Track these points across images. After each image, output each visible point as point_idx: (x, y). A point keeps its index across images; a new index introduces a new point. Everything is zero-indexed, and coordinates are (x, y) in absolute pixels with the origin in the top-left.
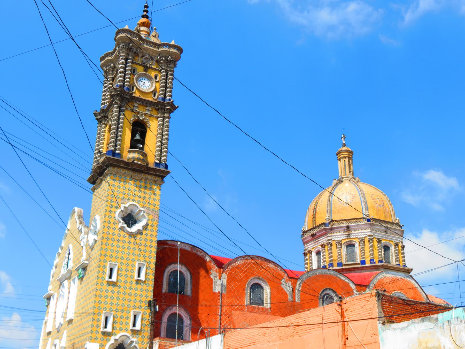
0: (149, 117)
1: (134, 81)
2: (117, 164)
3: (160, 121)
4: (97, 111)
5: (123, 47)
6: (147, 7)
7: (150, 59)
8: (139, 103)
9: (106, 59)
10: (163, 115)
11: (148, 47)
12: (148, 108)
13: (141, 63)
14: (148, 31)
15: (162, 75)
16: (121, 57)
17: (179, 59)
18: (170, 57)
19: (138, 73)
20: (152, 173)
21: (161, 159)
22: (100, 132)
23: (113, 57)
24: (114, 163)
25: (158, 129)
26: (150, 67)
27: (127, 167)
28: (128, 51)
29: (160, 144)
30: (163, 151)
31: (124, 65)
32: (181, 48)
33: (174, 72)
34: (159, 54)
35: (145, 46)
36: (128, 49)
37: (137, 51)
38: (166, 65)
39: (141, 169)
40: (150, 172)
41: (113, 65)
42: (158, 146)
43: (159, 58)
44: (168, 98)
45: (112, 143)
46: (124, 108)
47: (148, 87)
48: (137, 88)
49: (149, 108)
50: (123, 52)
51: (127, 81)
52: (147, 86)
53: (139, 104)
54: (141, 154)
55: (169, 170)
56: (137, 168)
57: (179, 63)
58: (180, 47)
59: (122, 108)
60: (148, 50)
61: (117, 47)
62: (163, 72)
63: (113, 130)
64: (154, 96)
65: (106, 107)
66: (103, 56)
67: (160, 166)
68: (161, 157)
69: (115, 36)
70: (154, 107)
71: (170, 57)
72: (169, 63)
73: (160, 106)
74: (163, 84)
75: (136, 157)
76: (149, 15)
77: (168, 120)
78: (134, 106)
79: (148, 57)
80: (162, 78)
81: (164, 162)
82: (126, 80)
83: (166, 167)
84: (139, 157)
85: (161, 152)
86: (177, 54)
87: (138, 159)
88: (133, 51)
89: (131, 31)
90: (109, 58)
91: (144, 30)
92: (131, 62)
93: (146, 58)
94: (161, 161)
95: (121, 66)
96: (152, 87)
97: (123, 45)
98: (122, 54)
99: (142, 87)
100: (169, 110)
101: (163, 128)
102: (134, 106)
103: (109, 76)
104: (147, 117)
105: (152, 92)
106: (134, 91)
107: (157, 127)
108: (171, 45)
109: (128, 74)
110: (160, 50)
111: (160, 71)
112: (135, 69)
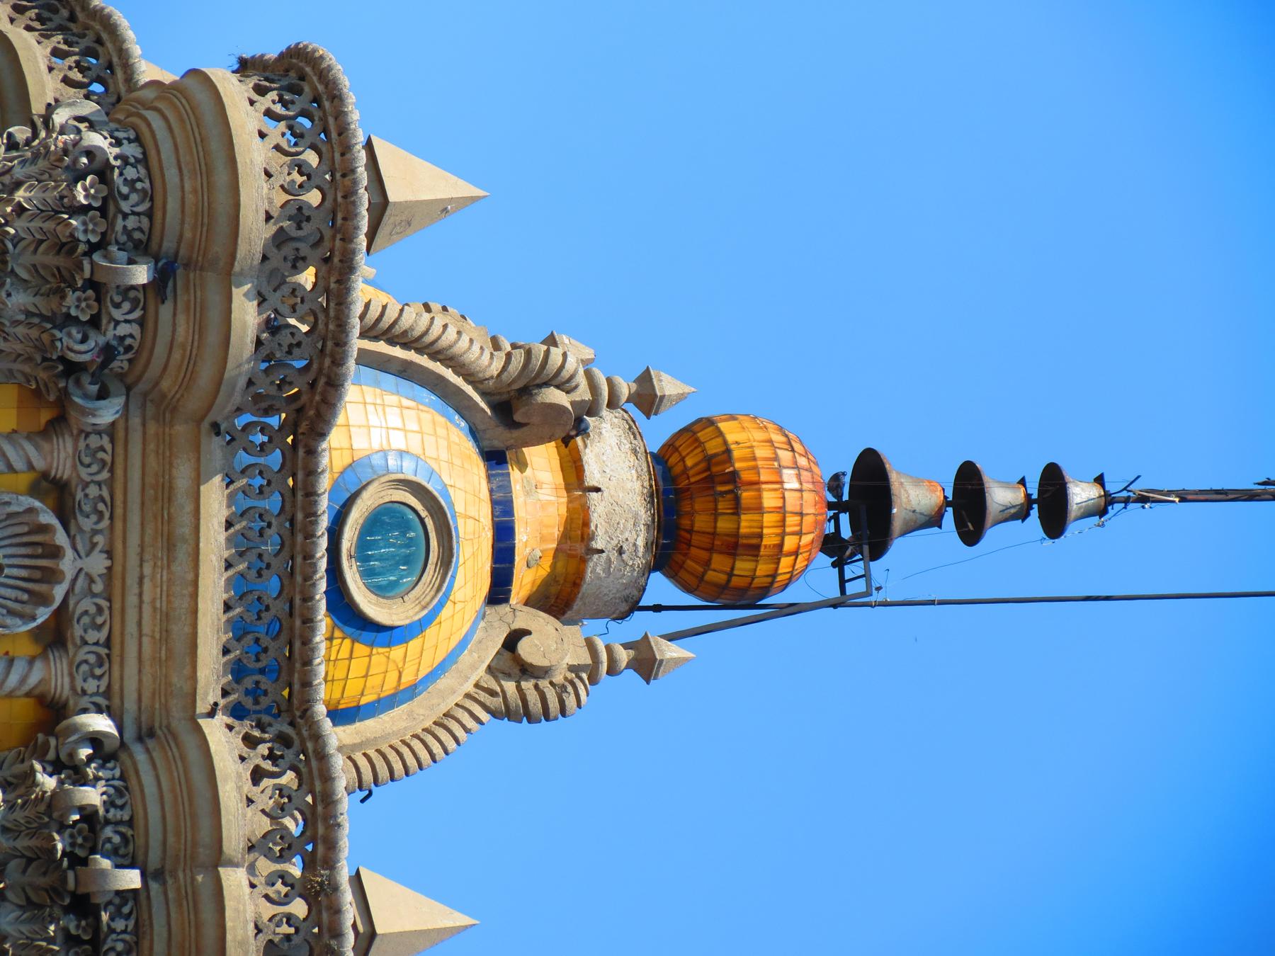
7: (44, 600)
14: (595, 567)
18: (131, 879)
36: (67, 246)
37: (103, 395)
43: (95, 740)
60: (170, 547)
71: (131, 879)
72: (55, 892)
79: (68, 564)
88: (69, 320)
91: (599, 508)
93: (55, 552)
97: (103, 173)
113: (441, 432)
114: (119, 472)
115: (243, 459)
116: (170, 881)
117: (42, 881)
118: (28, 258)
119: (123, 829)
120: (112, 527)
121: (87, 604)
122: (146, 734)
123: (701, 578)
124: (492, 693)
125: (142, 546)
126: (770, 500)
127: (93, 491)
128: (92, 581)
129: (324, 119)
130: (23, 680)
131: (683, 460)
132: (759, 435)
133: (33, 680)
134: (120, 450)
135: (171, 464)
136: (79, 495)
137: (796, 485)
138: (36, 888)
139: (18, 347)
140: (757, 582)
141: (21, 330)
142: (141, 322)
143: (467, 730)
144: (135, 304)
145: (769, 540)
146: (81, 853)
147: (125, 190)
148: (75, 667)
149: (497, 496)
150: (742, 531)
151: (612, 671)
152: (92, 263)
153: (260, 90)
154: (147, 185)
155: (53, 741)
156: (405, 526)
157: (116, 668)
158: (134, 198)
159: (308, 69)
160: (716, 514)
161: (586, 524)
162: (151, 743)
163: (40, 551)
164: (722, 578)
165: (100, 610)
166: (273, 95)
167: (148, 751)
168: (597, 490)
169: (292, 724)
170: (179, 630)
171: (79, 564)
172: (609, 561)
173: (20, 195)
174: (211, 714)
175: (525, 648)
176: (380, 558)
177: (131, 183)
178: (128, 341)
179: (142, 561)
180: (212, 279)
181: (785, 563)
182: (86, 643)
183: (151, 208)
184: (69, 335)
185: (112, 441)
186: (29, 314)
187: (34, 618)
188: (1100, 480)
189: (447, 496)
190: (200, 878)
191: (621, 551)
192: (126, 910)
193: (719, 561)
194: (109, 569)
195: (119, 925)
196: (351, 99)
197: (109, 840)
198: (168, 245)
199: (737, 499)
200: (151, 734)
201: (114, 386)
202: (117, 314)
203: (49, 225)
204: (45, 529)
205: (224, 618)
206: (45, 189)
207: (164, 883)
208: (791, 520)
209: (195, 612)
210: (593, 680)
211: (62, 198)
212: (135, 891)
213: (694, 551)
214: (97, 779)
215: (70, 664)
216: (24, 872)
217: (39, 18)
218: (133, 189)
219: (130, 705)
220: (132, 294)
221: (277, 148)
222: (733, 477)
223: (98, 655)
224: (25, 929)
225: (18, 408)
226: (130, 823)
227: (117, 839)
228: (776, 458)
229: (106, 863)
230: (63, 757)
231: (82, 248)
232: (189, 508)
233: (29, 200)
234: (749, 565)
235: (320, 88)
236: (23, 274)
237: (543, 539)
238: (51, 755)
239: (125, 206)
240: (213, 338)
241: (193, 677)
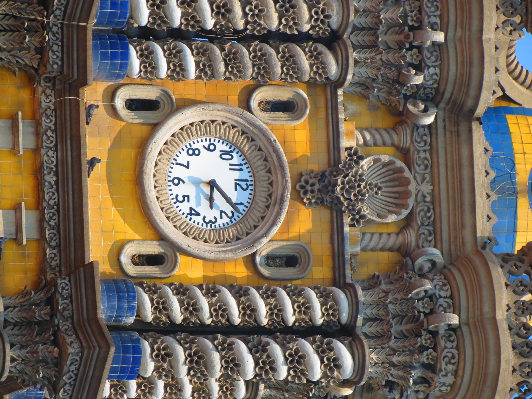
79: (412, 187)
127: (422, 155)
136: (416, 156)
223: (428, 230)
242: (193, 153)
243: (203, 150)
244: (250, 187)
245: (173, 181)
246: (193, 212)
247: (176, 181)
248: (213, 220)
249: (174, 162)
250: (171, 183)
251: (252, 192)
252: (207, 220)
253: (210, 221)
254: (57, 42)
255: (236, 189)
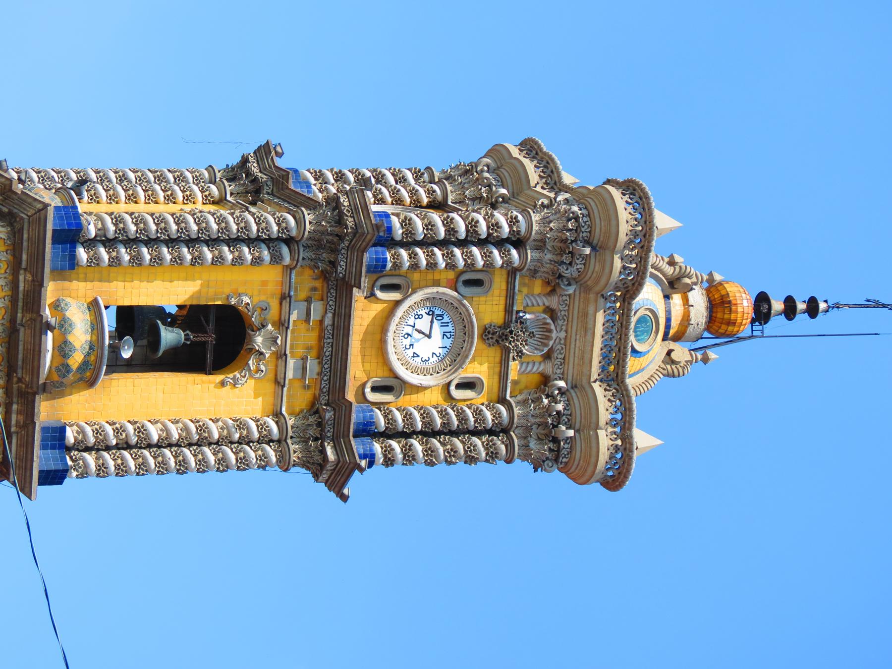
0: (271, 376)
1: (427, 286)
2: (24, 257)
3: (261, 426)
4: (280, 155)
5: (569, 220)
6: (812, 309)
7: (546, 345)
8: (328, 321)
9: (527, 162)
10: (290, 433)
11: (599, 330)
12: (312, 365)
13: (515, 308)
14: (690, 328)
15: (484, 408)
16: (520, 217)
17: (575, 479)
18: (571, 433)
19: (465, 302)
20: (14, 418)
21: (88, 449)
22: (185, 180)
23: (538, 189)
24: (25, 244)
25: (225, 423)
26: (508, 351)
27: (20, 304)
28: (558, 244)
29: (155, 438)
30: (126, 454)
31: (489, 235)
32: (626, 477)
33: (509, 461)
34: (580, 386)
35: (600, 318)
36: (564, 241)
37: (569, 284)
38: (532, 420)
39: (20, 363)
40: (15, 407)
41: (503, 196)
42: (141, 430)
43: (559, 389)
44: (377, 447)
45: (116, 225)
46: (287, 260)
47: (415, 355)
48: (397, 303)
49: (317, 369)
50: (545, 221)
51: (416, 254)
52: (416, 349)
53: (321, 322)
54: (93, 358)
55: (43, 492)
56: (21, 347)
57: (556, 478)
58: (628, 471)
59: (285, 250)
60: (586, 331)
61: (567, 195)
62: (497, 415)
63: (177, 224)
64: (375, 389)
65: (305, 192)
66: (541, 150)
67: (53, 447)
68: (98, 450)
69: (620, 180)
70: (321, 390)
71: (571, 433)
72: (546, 435)
73: (329, 415)
74: (438, 421)
75: (70, 338)
76: (777, 323)
77: (274, 459)
78: (308, 300)
79: (554, 335)
80: (469, 412)
81: (70, 463)
82: (418, 250)
83: (54, 477)
84: (72, 348)
85: (118, 447)
86: (593, 460)
87: (63, 349)
88: (563, 263)
89: (650, 242)
90: (533, 174)
92: (508, 263)
93: (550, 331)
94: (74, 453)
95: (477, 222)
96: (416, 370)
97: (576, 219)
98: (536, 218)
99: (409, 330)
100: (318, 458)
101: (232, 443)
102: (308, 300)
103: (449, 188)
104: (272, 366)
105: (397, 377)
106: (380, 294)
107: (233, 417)
108: (630, 429)
109: (450, 256)
110: (596, 386)
111: (502, 400)
112: (487, 284)
113: (656, 292)
114: (571, 307)
115: (609, 305)
116: (581, 433)
117: (543, 432)
118: (551, 244)
119: (568, 417)
120: (567, 324)
121: (559, 347)
122: (574, 387)
123: (717, 331)
124: (664, 369)
125: (577, 330)
126: (740, 309)
127: (563, 313)
128: (560, 340)
129: (643, 204)
130: (538, 369)
131: (714, 295)
132: (736, 289)
133: (541, 369)
134: (572, 301)
135: (588, 306)
136: (559, 314)
137: (747, 305)
138: (541, 434)
139: (545, 270)
140: (733, 333)
141: (548, 266)
142: (584, 264)
143: (657, 381)
144: (583, 258)
145: (739, 321)
146: (555, 424)
147: (583, 224)
148: (554, 366)
149: (667, 309)
150: (732, 318)
151: (696, 362)
152: (572, 246)
153: (624, 194)
154: (590, 223)
155: (547, 389)
156: (646, 322)
157: (566, 366)
158: (586, 227)
159: (637, 188)
160: (724, 313)
161: (689, 316)
162: (576, 390)
163: (545, 330)
164: (723, 331)
165: (562, 348)
166: (627, 196)
167: (575, 392)
168: (692, 306)
169: (618, 385)
170: (587, 356)
171: (557, 335)
172: (694, 327)
173: (552, 225)
174: (595, 382)
175: (673, 355)
176: (640, 331)
177: (585, 222)
178: (580, 270)
179: (576, 335)
180: (608, 253)
181: (742, 327)
182: (557, 358)
183: (590, 231)
184: (563, 267)
185: (570, 298)
186: (551, 261)
187: (543, 351)
188: (826, 301)
189: (658, 312)
190: (591, 433)
191: (698, 324)
192: (568, 441)
193: (724, 327)
194: (566, 336)
195: (566, 446)
196: (652, 199)
197: (564, 420)
198: (595, 242)
199: (731, 309)
200: (576, 387)
201: (572, 282)
202: (578, 262)
203: (559, 234)
204: (548, 324)
205: (600, 352)
206: (559, 223)
207: (580, 434)
208: (745, 315)
209: (592, 351)
210: (691, 364)
211: (564, 226)
212: (571, 437)
213: (716, 324)
214: (561, 401)
215: (553, 365)
216: (537, 428)
217: (527, 154)
218: (586, 224)
219: (570, 378)
220: (582, 256)
221: (630, 213)
222: (730, 302)
223: (561, 362)
224: (538, 447)
225: (542, 286)
226: (570, 415)
227: (566, 420)
228: (742, 297)
229: (564, 428)
230: (549, 393)
231: (569, 241)
232: (593, 320)
233: (554, 226)
234: (733, 328)
235: (642, 194)
236: (550, 248)
237: (677, 321)
238: (546, 393)
239: (583, 230)
240: (607, 270)
241: (590, 371)
242: (419, 318)
243: (425, 315)
244: (452, 337)
245: (404, 336)
246: (415, 355)
247: (406, 336)
248: (427, 359)
249: (406, 324)
250: (403, 338)
251: (453, 340)
252: (423, 360)
253: (426, 360)
254: (343, 259)
255: (443, 338)
